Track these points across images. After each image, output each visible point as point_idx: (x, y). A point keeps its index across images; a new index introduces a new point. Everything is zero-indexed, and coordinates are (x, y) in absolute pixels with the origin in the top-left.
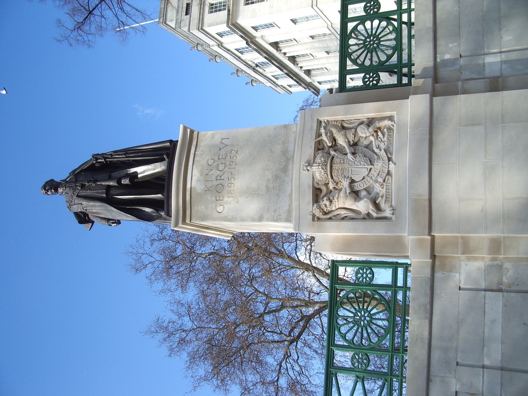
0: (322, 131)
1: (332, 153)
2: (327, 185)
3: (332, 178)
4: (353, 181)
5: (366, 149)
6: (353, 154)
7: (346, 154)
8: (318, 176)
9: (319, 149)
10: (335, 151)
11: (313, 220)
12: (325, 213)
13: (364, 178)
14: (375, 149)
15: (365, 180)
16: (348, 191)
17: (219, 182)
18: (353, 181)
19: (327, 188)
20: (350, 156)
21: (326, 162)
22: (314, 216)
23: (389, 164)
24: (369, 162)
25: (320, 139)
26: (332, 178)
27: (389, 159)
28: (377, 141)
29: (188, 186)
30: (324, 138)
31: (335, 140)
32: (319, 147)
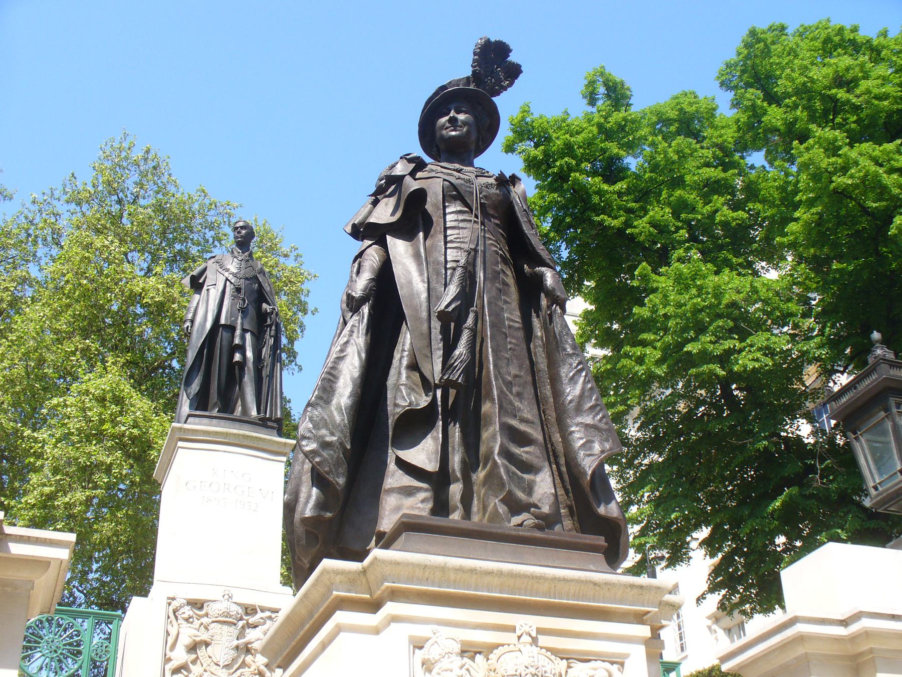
0: (268, 614)
1: (241, 623)
2: (207, 615)
3: (213, 622)
6: (237, 647)
7: (238, 639)
9: (246, 609)
10: (243, 627)
11: (169, 598)
12: (174, 612)
14: (241, 670)
16: (198, 639)
18: (207, 644)
19: (202, 616)
20: (236, 643)
22: (173, 599)
24: (226, 663)
25: (259, 611)
26: (213, 622)
30: (260, 615)
31: (256, 627)
32: (250, 610)
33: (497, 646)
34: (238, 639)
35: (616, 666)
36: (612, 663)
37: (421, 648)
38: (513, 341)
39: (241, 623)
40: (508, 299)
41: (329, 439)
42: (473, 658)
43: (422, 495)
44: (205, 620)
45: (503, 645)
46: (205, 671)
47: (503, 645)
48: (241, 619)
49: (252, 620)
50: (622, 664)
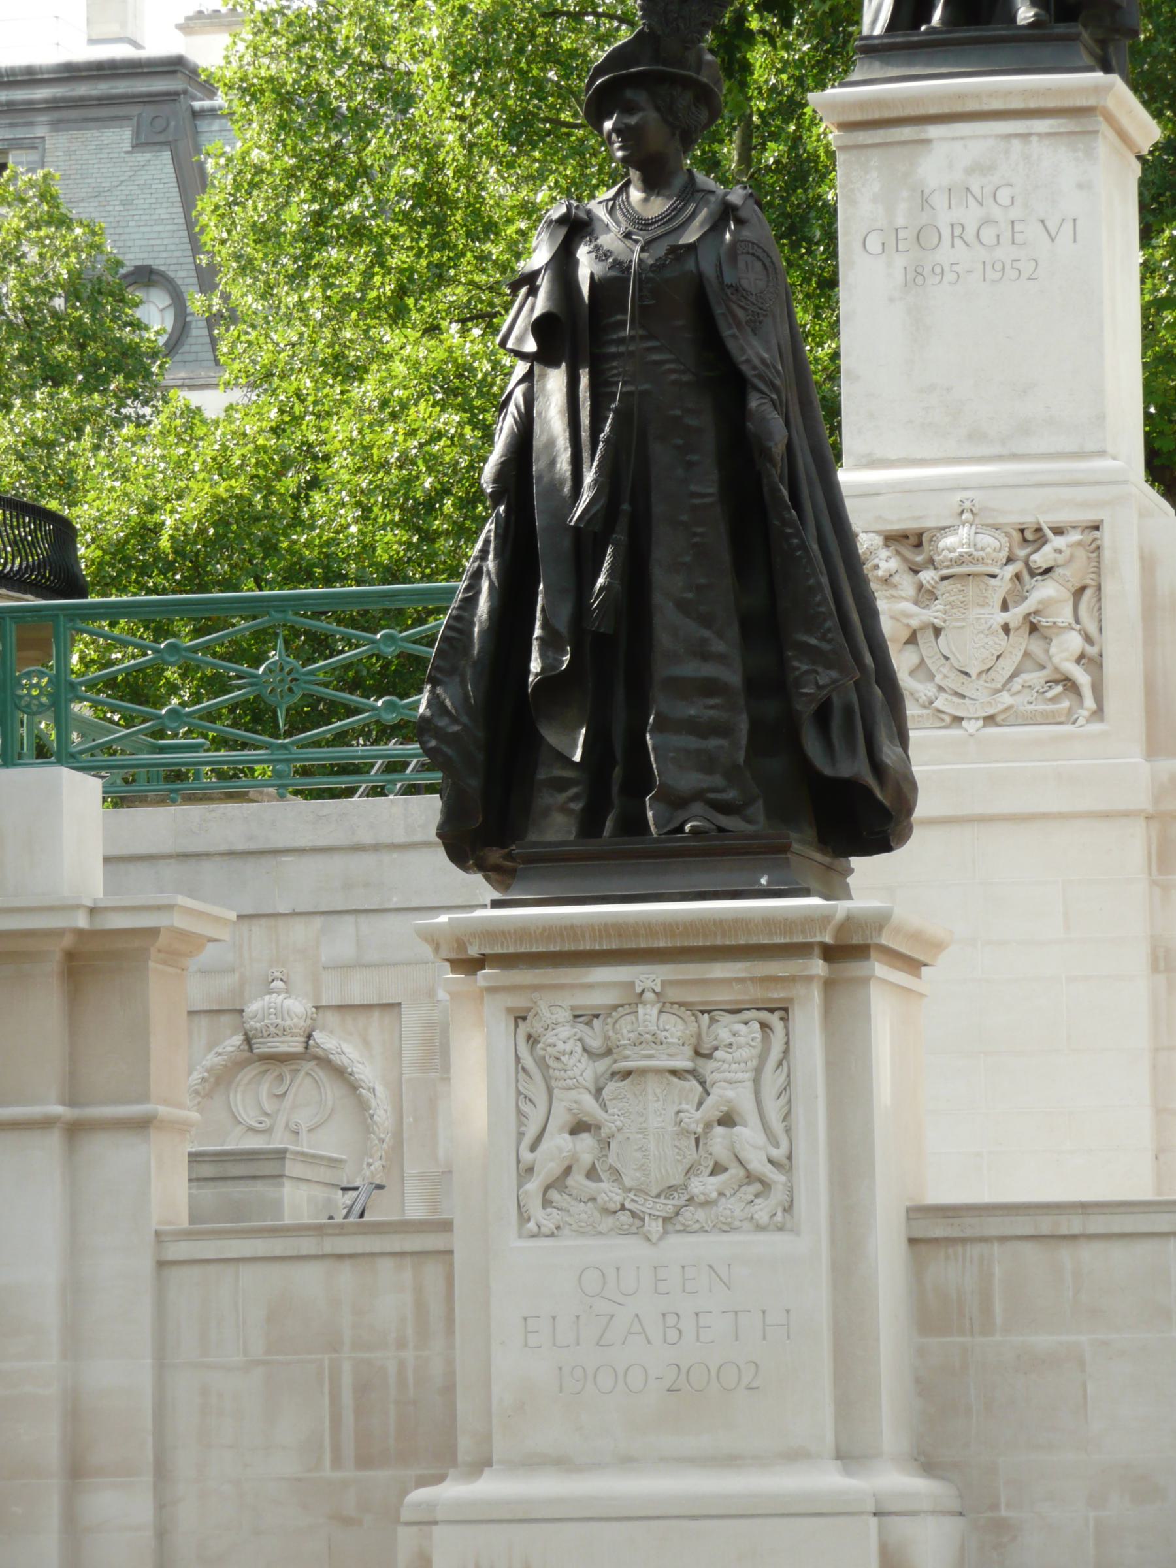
1: (1011, 570)
2: (931, 563)
4: (937, 631)
5: (1021, 653)
6: (1006, 629)
8: (948, 541)
10: (1018, 576)
13: (947, 658)
15: (943, 661)
16: (914, 623)
17: (946, 233)
18: (937, 631)
21: (980, 561)
23: (977, 719)
27: (990, 720)
28: (1043, 682)
29: (934, 131)
33: (616, 1007)
34: (1005, 607)
35: (777, 1014)
36: (771, 1011)
37: (524, 1018)
38: (700, 530)
39: (1011, 570)
40: (695, 458)
41: (456, 728)
42: (589, 1024)
43: (573, 791)
44: (928, 576)
45: (622, 1006)
46: (941, 689)
47: (622, 1006)
48: (1010, 560)
49: (1041, 559)
50: (786, 1010)
